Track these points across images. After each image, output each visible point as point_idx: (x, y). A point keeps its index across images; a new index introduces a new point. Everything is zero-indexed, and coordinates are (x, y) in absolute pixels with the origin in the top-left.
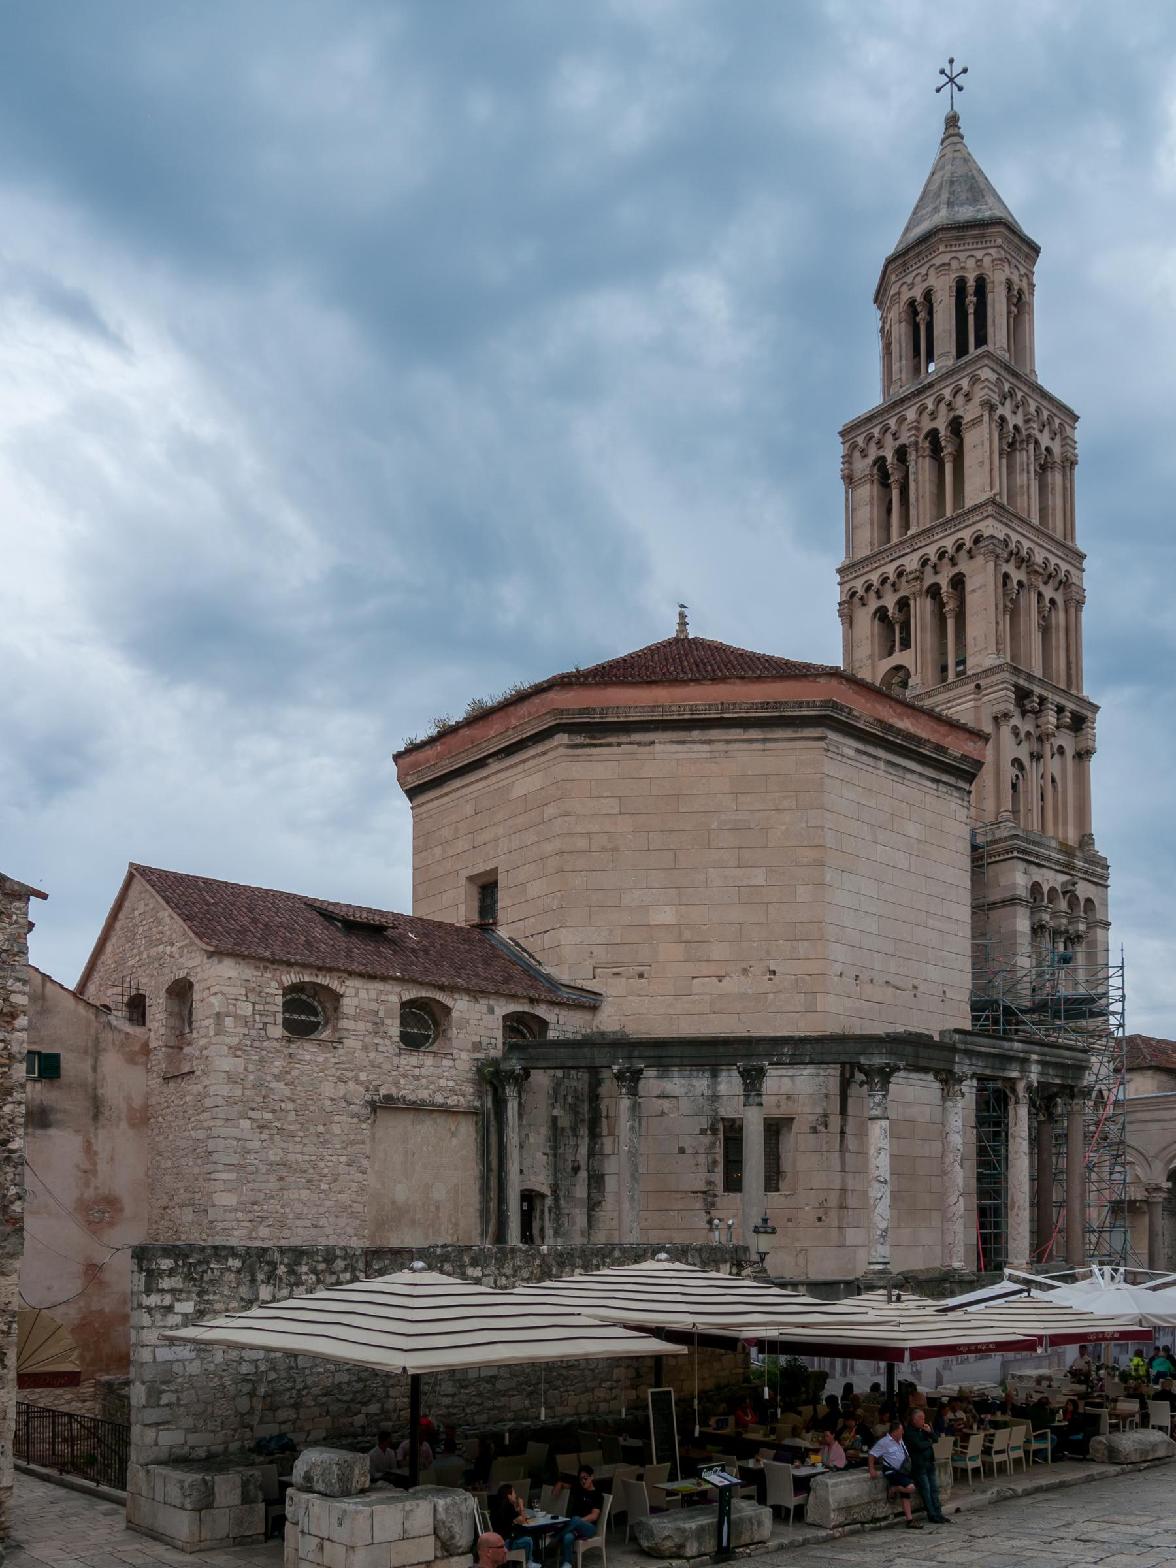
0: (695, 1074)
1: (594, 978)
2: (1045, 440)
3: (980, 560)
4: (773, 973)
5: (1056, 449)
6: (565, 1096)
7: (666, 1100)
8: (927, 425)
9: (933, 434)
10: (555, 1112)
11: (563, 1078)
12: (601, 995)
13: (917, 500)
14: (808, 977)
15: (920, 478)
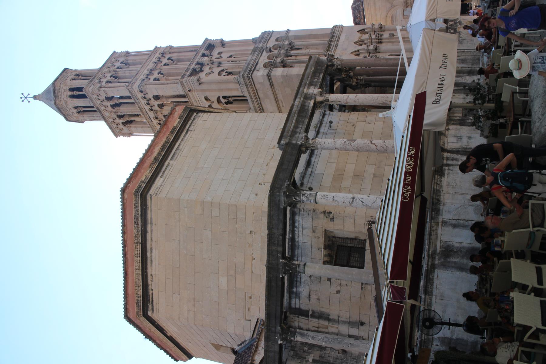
0: (299, 279)
1: (250, 320)
2: (118, 64)
3: (148, 91)
4: (251, 232)
5: (121, 60)
6: (304, 351)
7: (311, 296)
8: (110, 109)
9: (113, 106)
10: (311, 360)
11: (294, 351)
12: (258, 319)
13: (133, 112)
14: (254, 214)
15: (126, 111)
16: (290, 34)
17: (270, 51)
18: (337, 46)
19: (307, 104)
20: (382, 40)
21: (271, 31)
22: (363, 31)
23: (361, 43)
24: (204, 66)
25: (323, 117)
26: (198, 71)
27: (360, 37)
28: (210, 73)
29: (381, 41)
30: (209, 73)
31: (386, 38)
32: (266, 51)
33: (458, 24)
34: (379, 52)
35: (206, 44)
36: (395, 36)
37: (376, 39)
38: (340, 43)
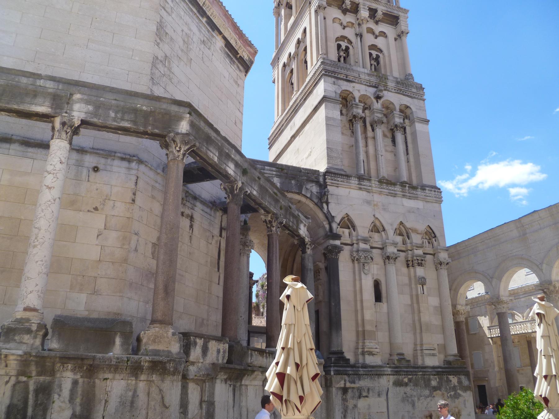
16: (419, 126)
17: (378, 98)
18: (392, 196)
19: (39, 100)
20: (413, 266)
21: (425, 97)
22: (433, 235)
23: (405, 234)
24: (355, 15)
25: (123, 159)
26: (343, 7)
27: (415, 231)
28: (341, 24)
29: (410, 265)
30: (342, 23)
31: (415, 272)
32: (376, 92)
33: (452, 393)
34: (385, 262)
35: (396, 12)
36: (420, 286)
37: (412, 257)
38: (399, 200)
